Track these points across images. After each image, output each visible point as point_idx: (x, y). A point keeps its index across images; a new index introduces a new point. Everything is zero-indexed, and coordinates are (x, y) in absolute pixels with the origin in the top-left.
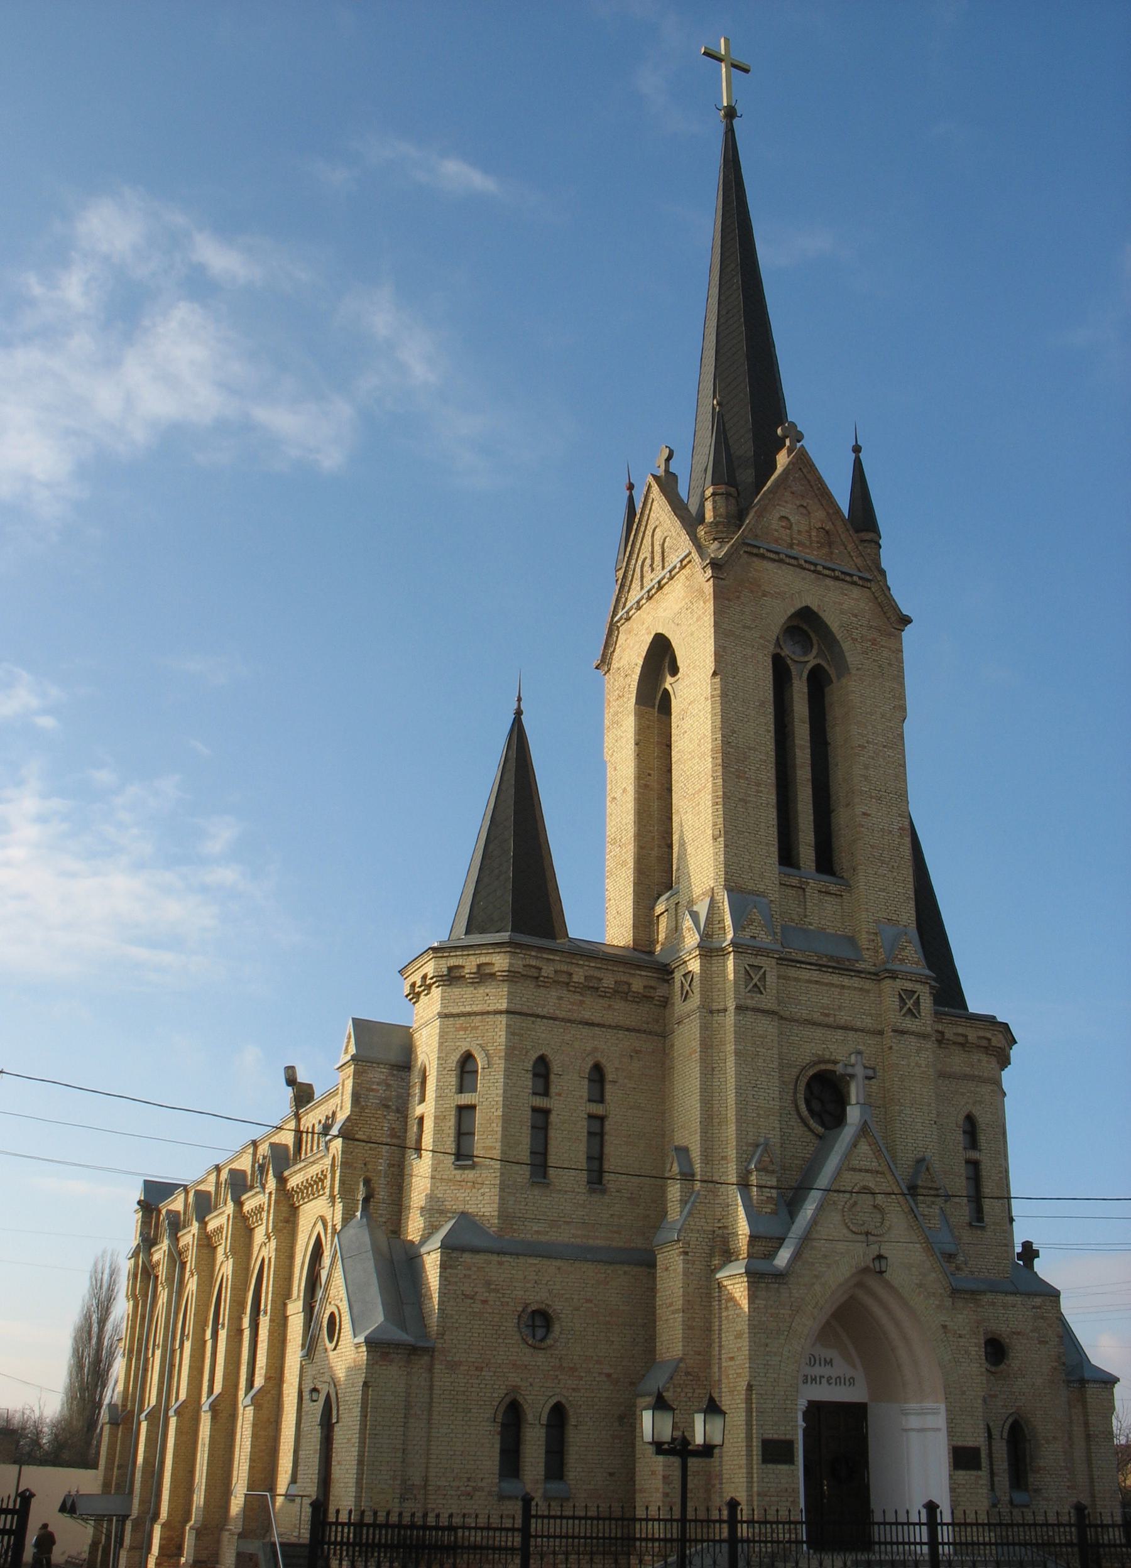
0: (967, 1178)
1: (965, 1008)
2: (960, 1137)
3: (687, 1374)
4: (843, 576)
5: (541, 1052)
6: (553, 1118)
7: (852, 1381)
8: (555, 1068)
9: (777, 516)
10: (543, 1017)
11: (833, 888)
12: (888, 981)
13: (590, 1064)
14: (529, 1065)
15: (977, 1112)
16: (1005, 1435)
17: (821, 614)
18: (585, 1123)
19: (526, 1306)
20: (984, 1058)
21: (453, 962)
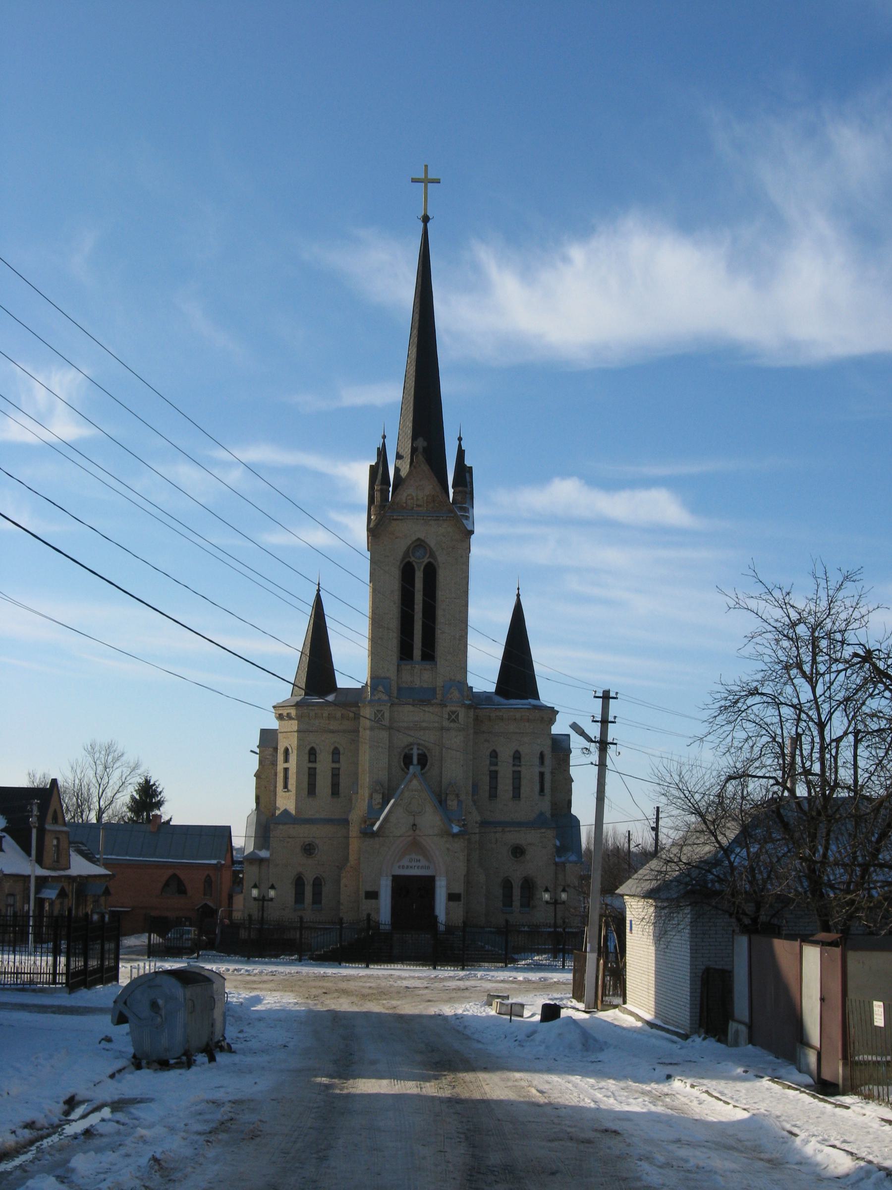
0: (514, 779)
1: (536, 696)
2: (511, 760)
3: (352, 867)
4: (437, 518)
5: (311, 746)
6: (318, 771)
7: (428, 868)
8: (318, 751)
9: (406, 495)
10: (312, 732)
11: (428, 667)
12: (444, 708)
13: (332, 747)
14: (307, 751)
15: (520, 750)
16: (520, 885)
17: (426, 540)
18: (330, 772)
19: (304, 842)
20: (527, 724)
21: (280, 712)
